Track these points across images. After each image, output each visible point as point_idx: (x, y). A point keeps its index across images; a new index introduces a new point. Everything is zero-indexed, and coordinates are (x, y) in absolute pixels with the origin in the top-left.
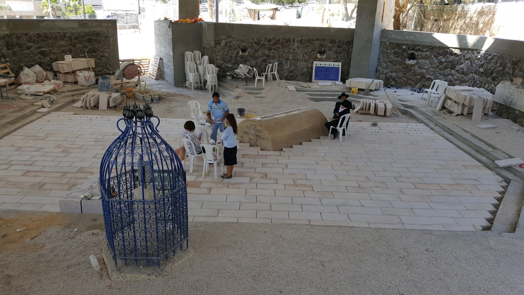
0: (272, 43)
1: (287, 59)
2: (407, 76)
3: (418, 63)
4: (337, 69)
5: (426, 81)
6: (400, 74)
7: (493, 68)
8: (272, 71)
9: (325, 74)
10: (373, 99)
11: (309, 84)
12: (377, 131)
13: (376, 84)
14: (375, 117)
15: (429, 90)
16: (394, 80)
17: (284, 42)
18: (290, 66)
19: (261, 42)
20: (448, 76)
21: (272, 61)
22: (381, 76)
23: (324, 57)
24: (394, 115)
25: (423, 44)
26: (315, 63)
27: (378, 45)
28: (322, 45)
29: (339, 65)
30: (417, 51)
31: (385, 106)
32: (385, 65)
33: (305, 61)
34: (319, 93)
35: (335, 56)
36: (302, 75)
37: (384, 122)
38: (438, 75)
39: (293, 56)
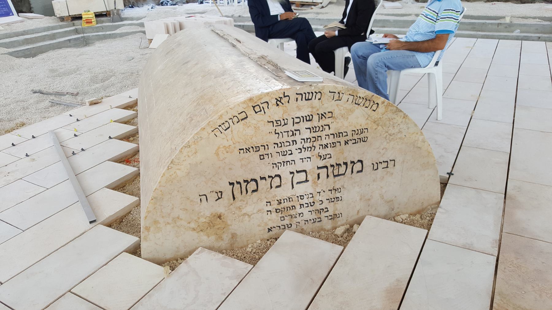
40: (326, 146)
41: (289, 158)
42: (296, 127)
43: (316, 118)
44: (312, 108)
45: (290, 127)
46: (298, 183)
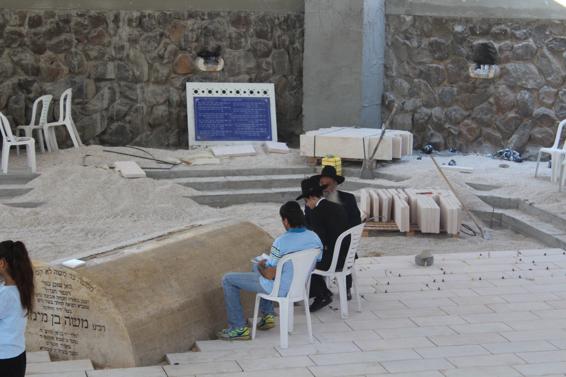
0: (43, 29)
1: (100, 79)
2: (477, 112)
3: (504, 73)
4: (263, 104)
5: (534, 125)
6: (457, 111)
8: (53, 117)
9: (226, 120)
10: (396, 188)
11: (181, 154)
12: (439, 278)
13: (395, 143)
14: (415, 239)
15: (553, 150)
16: (439, 127)
17: (83, 25)
18: (112, 100)
19: (8, 28)
21: (48, 86)
22: (399, 119)
23: (220, 67)
24: (467, 232)
25: (515, 16)
26: (191, 86)
27: (380, 24)
28: (207, 32)
29: (266, 90)
30: (497, 37)
31: (438, 202)
32: (406, 85)
33: (158, 82)
34: (221, 179)
35: (252, 64)
36: (152, 126)
37: (449, 251)
39: (119, 68)
40: (69, 305)
41: (51, 305)
42: (54, 288)
43: (63, 286)
44: (62, 280)
45: (51, 287)
46: (55, 323)
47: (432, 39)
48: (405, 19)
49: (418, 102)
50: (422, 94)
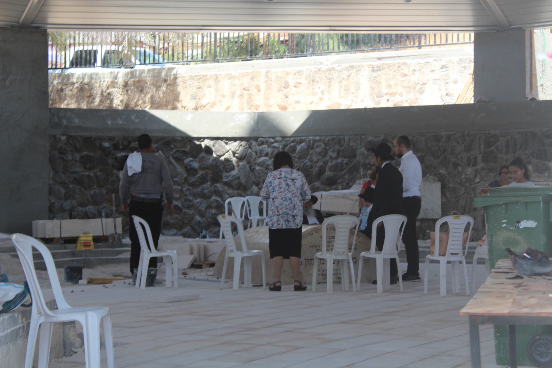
7: (320, 164)
20: (210, 197)
32: (63, 190)
38: (191, 198)
47: (84, 153)
48: (60, 139)
49: (74, 203)
50: (77, 196)
